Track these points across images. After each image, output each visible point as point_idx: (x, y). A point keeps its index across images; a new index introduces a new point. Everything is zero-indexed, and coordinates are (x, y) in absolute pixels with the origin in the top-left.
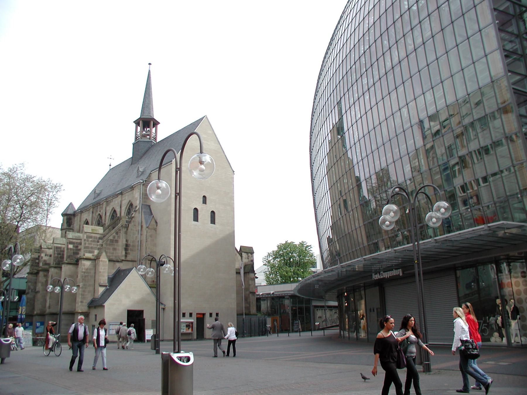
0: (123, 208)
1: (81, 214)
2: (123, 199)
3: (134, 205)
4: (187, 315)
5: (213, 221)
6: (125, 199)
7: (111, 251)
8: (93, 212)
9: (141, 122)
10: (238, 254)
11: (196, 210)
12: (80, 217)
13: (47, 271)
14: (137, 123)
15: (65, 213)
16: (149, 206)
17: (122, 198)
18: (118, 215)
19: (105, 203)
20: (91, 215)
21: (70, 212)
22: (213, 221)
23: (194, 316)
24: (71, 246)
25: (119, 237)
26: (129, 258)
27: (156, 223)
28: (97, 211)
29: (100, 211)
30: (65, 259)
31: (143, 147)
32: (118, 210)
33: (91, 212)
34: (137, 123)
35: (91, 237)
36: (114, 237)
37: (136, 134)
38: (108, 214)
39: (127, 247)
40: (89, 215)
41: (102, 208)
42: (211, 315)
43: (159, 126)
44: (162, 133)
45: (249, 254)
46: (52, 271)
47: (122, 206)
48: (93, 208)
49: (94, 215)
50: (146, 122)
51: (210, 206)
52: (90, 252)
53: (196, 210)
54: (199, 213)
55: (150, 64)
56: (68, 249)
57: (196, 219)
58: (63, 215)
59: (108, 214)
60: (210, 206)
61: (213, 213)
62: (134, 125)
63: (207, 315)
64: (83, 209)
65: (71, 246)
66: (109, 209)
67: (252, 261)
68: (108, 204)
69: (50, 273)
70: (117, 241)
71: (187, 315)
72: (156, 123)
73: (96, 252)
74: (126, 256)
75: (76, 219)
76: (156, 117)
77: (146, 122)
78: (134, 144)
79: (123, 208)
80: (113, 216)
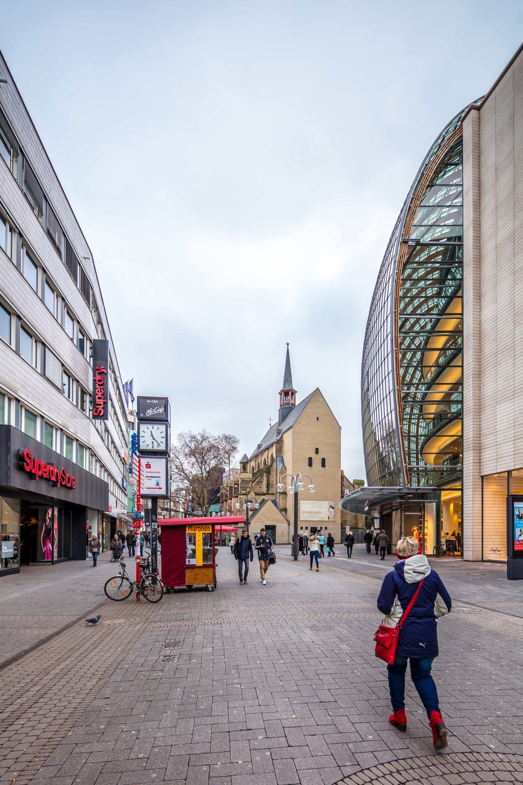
4: (304, 528)
5: (323, 465)
7: (258, 488)
11: (310, 459)
13: (226, 501)
16: (282, 457)
21: (245, 461)
22: (323, 465)
23: (309, 529)
24: (236, 486)
25: (263, 479)
26: (270, 492)
31: (286, 410)
35: (244, 481)
36: (260, 479)
37: (280, 403)
44: (299, 399)
46: (229, 501)
50: (288, 393)
51: (321, 455)
52: (244, 490)
53: (310, 459)
57: (310, 464)
58: (241, 463)
60: (321, 455)
61: (323, 460)
65: (236, 486)
68: (262, 456)
70: (262, 482)
71: (304, 528)
73: (248, 490)
74: (268, 491)
76: (295, 387)
77: (288, 393)
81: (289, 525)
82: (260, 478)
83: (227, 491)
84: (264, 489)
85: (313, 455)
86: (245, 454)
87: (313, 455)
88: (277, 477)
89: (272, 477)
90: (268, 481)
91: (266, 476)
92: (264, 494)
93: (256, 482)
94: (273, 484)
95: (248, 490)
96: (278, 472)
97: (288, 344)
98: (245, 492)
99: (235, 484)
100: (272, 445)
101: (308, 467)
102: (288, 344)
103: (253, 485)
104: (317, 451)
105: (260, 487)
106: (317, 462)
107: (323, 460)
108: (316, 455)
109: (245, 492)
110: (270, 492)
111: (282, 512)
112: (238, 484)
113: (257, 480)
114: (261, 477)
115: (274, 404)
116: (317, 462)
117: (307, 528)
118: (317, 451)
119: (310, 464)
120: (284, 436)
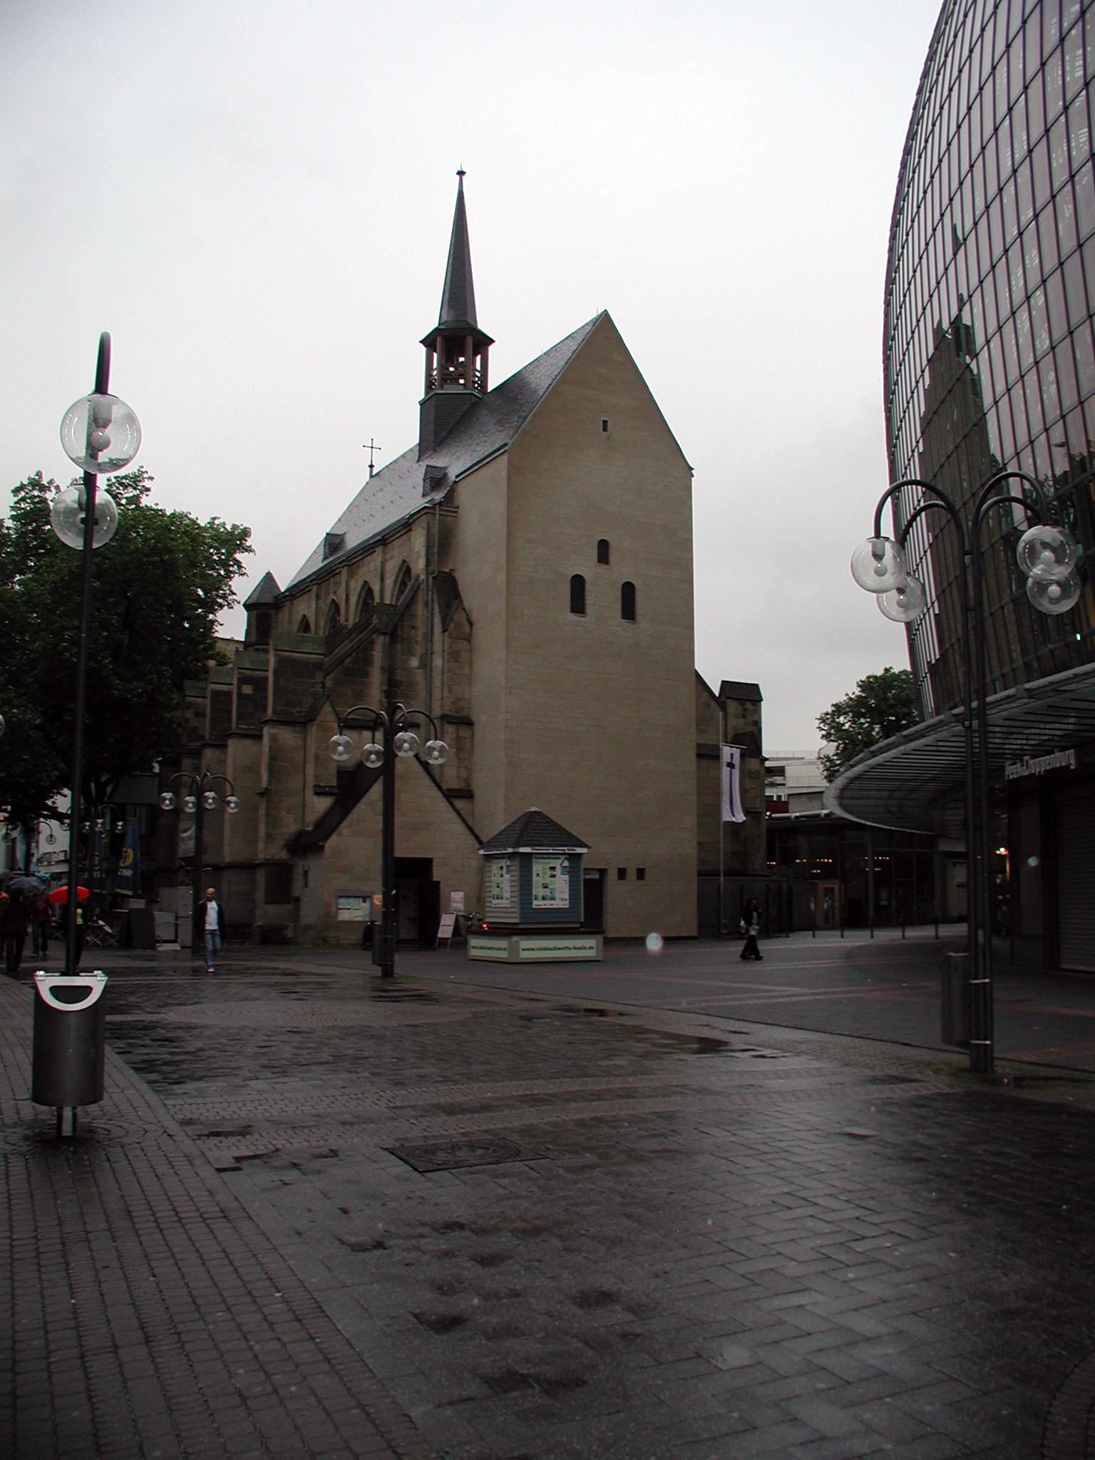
0: (389, 582)
1: (292, 601)
2: (388, 556)
3: (414, 573)
5: (629, 612)
6: (392, 558)
8: (318, 598)
9: (439, 339)
10: (713, 705)
11: (578, 583)
12: (291, 611)
14: (429, 342)
15: (253, 601)
17: (384, 553)
18: (377, 600)
19: (344, 571)
20: (314, 603)
21: (269, 599)
22: (629, 612)
24: (248, 690)
28: (327, 594)
29: (335, 593)
30: (234, 724)
32: (376, 588)
33: (314, 597)
34: (429, 342)
38: (353, 600)
39: (393, 688)
40: (310, 606)
41: (338, 583)
42: (622, 873)
43: (491, 348)
44: (501, 367)
45: (749, 705)
46: (209, 754)
47: (387, 574)
49: (321, 602)
50: (457, 339)
51: (621, 570)
53: (578, 583)
54: (588, 587)
56: (240, 695)
57: (578, 605)
59: (353, 600)
60: (621, 570)
61: (628, 591)
62: (424, 349)
63: (612, 876)
64: (298, 589)
65: (248, 690)
66: (356, 586)
67: (757, 724)
68: (352, 574)
69: (204, 762)
72: (483, 343)
75: (280, 617)
76: (484, 325)
77: (457, 339)
78: (422, 404)
79: (389, 582)
80: (366, 604)
83: (200, 714)
85: (587, 567)
87: (587, 567)
94: (411, 685)
97: (461, 173)
99: (243, 680)
100: (406, 525)
102: (461, 173)
103: (329, 683)
106: (604, 597)
107: (628, 591)
111: (459, 804)
112: (260, 684)
115: (406, 378)
116: (604, 597)
119: (578, 605)
120: (461, 488)
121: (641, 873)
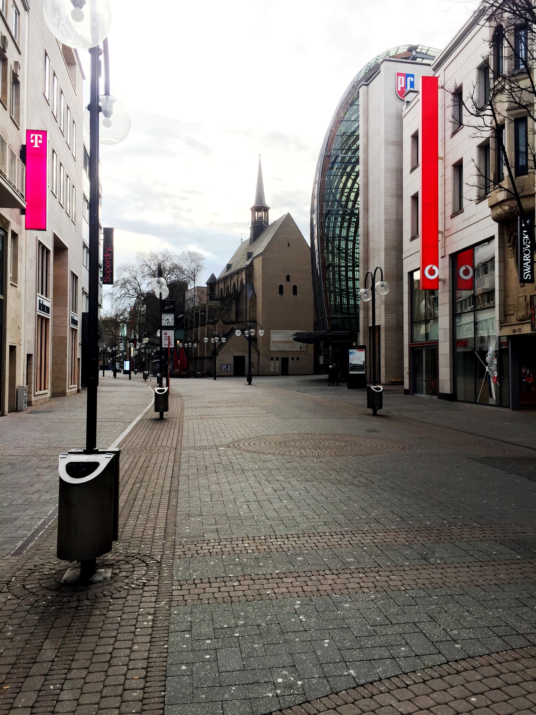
11: (281, 287)
13: (192, 328)
16: (252, 284)
21: (213, 282)
23: (280, 359)
24: (203, 314)
25: (232, 307)
27: (256, 296)
35: (212, 309)
36: (228, 307)
38: (232, 286)
39: (237, 314)
42: (293, 359)
46: (194, 329)
48: (224, 280)
50: (261, 207)
51: (293, 283)
52: (212, 319)
53: (281, 287)
55: (260, 155)
59: (232, 286)
60: (293, 283)
61: (295, 288)
63: (290, 359)
65: (203, 314)
70: (231, 310)
77: (261, 207)
81: (259, 355)
82: (228, 305)
84: (233, 317)
85: (284, 283)
86: (213, 275)
87: (284, 283)
88: (246, 304)
89: (242, 304)
90: (237, 309)
91: (236, 304)
92: (233, 323)
93: (224, 310)
95: (216, 318)
96: (248, 299)
98: (212, 320)
99: (202, 311)
101: (279, 296)
103: (221, 313)
104: (288, 278)
105: (229, 315)
107: (295, 288)
108: (288, 283)
109: (212, 320)
110: (239, 320)
112: (205, 312)
113: (226, 308)
114: (230, 305)
117: (277, 359)
118: (288, 278)
121: (298, 359)
